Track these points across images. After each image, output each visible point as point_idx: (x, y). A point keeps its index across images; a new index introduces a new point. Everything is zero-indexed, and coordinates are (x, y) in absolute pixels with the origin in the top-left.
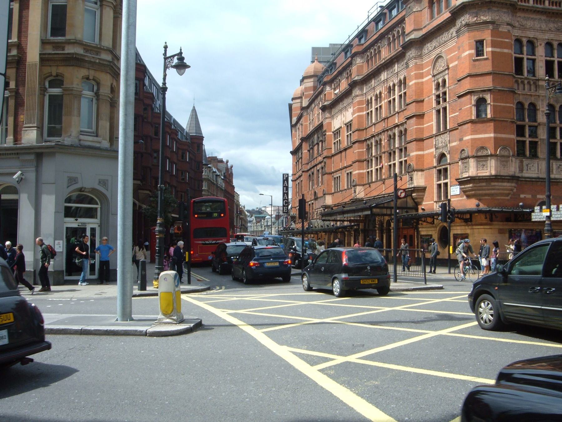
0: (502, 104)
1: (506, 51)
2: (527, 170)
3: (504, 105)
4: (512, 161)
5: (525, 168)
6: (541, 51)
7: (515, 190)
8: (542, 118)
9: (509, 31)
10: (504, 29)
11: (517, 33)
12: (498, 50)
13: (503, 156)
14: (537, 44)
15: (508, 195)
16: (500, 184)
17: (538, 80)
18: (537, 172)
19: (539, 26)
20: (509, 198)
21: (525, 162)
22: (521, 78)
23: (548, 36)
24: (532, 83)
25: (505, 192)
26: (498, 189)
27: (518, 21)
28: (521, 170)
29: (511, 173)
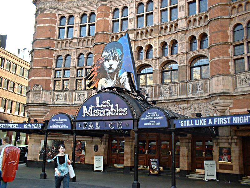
0: (40, 58)
1: (47, 25)
2: (57, 99)
3: (42, 58)
4: (43, 93)
5: (56, 98)
6: (77, 21)
7: (48, 113)
8: (73, 64)
9: (51, 12)
10: (47, 12)
11: (61, 13)
12: (42, 25)
13: (36, 91)
14: (75, 16)
15: (43, 116)
16: (33, 109)
17: (73, 39)
18: (64, 100)
19: (76, 5)
20: (43, 118)
21: (56, 94)
22: (61, 40)
23: (82, 10)
24: (69, 41)
25: (38, 114)
26: (33, 112)
27: (63, 5)
28: (53, 100)
29: (40, 102)
